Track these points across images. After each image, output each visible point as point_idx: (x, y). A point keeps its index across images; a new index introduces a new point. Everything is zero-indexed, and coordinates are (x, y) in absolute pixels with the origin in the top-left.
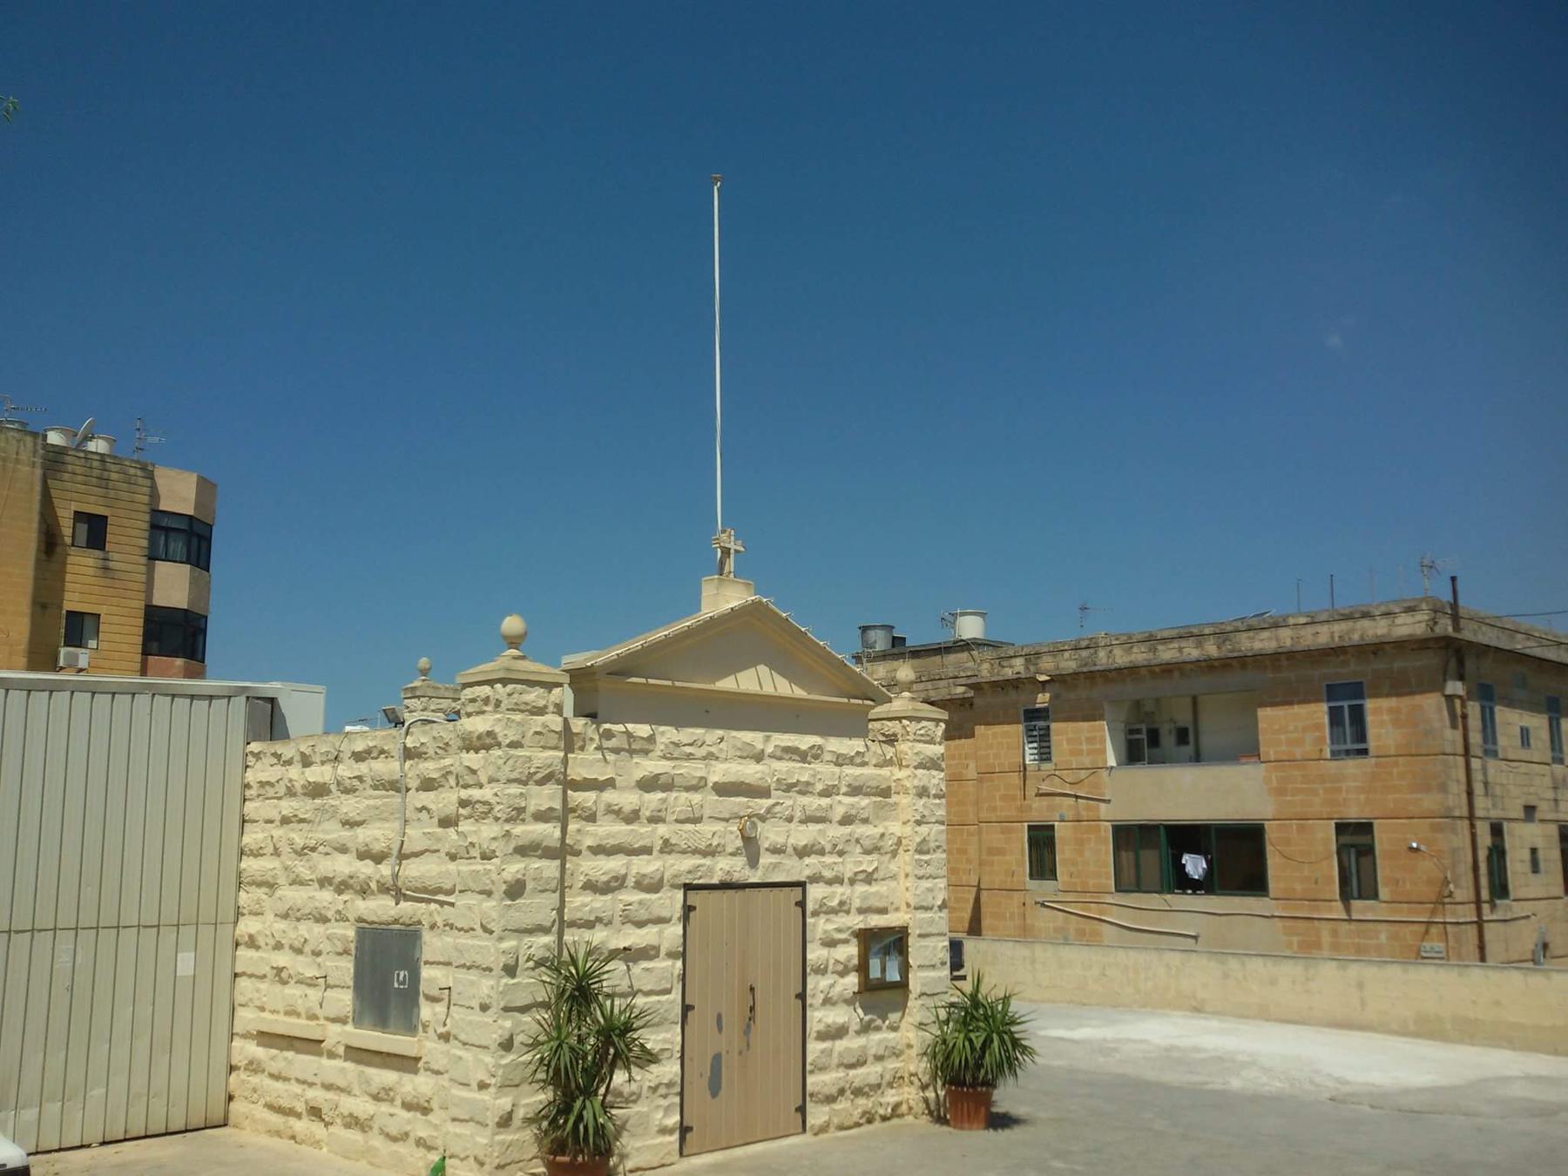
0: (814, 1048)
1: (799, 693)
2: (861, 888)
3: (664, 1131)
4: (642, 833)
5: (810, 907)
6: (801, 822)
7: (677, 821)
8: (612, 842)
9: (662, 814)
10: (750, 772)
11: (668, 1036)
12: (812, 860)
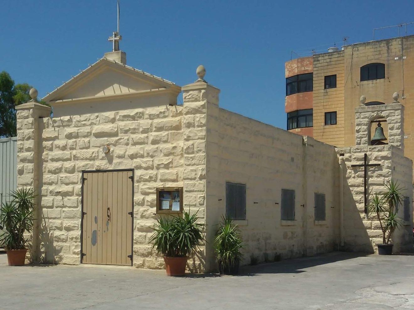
0: (137, 234)
1: (132, 91)
2: (162, 171)
3: (74, 253)
4: (67, 153)
5: (136, 179)
6: (132, 145)
7: (81, 149)
8: (56, 157)
9: (74, 146)
10: (107, 127)
11: (77, 222)
12: (138, 160)
